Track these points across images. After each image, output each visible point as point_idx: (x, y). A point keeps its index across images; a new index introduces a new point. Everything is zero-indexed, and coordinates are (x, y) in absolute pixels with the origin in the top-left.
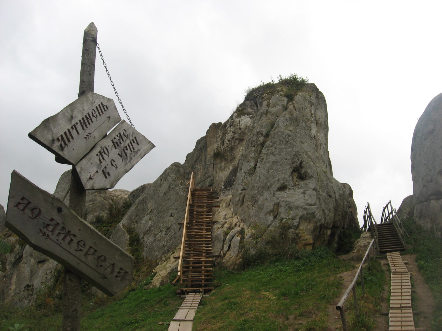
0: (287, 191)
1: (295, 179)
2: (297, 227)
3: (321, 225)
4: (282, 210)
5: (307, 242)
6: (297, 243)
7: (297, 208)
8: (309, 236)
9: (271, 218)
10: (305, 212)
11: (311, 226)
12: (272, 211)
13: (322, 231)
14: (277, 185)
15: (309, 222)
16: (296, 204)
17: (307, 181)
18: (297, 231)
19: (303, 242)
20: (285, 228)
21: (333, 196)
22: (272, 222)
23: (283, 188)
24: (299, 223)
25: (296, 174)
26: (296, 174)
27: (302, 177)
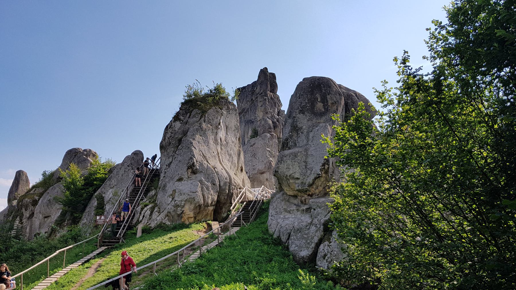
0: (183, 182)
1: (189, 174)
2: (183, 207)
3: (199, 205)
4: (177, 194)
5: (189, 216)
6: (182, 217)
7: (184, 194)
8: (189, 213)
9: (171, 199)
10: (188, 197)
11: (192, 207)
12: (171, 195)
13: (202, 209)
14: (177, 178)
15: (191, 204)
16: (184, 191)
17: (197, 175)
18: (183, 209)
19: (187, 216)
20: (177, 206)
21: (218, 184)
22: (171, 201)
23: (180, 180)
24: (185, 204)
25: (190, 170)
26: (190, 170)
27: (194, 172)
